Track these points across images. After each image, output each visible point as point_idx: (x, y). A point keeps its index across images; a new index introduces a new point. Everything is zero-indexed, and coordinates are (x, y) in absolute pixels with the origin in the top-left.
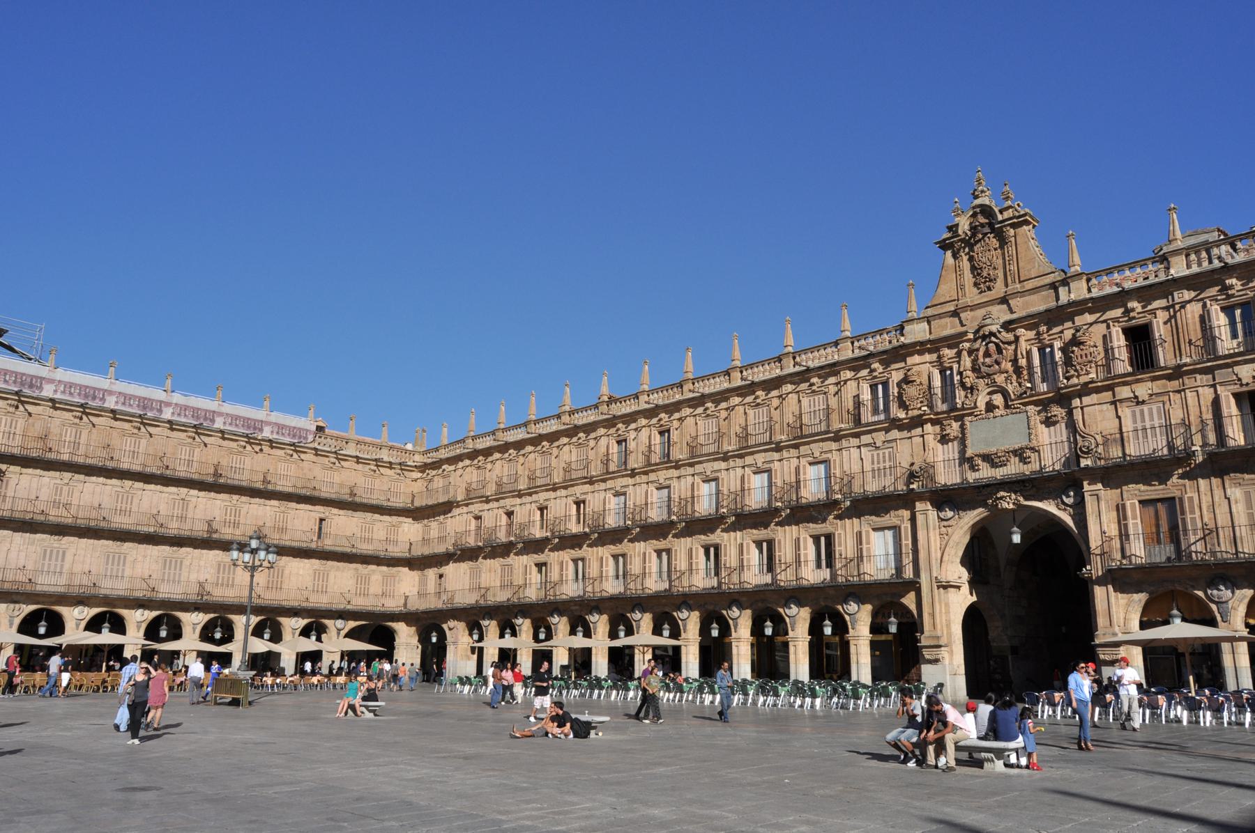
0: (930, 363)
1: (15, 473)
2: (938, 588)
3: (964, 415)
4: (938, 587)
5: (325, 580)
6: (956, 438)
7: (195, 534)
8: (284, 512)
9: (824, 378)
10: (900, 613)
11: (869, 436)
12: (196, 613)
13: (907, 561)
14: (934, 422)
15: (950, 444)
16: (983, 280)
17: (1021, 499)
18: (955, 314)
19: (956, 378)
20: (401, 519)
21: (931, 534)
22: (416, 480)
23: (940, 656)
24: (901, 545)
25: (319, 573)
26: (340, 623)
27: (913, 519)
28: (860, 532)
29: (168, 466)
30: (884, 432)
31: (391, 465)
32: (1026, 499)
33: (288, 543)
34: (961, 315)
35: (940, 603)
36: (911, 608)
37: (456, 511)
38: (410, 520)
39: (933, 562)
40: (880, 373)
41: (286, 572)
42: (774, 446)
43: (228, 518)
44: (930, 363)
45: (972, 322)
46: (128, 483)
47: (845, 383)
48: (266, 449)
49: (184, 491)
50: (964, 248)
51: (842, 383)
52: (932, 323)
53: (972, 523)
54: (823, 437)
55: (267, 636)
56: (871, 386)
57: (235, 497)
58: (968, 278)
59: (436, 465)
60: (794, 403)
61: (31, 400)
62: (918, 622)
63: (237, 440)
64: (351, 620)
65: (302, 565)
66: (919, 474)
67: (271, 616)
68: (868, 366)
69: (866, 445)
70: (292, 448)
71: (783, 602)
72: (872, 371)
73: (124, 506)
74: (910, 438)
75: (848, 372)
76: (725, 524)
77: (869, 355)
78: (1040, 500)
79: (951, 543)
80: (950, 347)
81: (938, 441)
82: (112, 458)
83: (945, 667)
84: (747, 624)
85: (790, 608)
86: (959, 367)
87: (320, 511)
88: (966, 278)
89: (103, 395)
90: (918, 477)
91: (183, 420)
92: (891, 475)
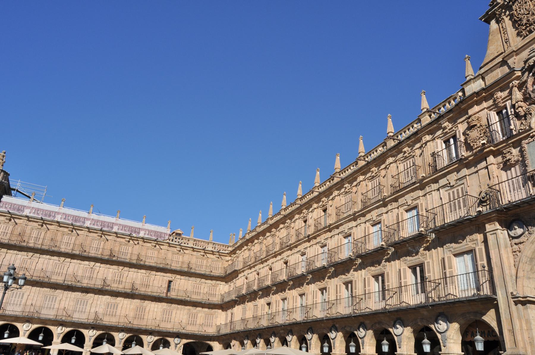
0: (487, 108)
1: (4, 252)
2: (516, 305)
3: (521, 139)
4: (516, 303)
5: (170, 315)
6: (517, 162)
7: (96, 287)
8: (148, 276)
9: (411, 146)
10: (486, 332)
11: (445, 179)
12: (92, 330)
13: (484, 278)
14: (496, 154)
15: (513, 169)
16: (524, 28)
18: (504, 63)
19: (511, 111)
20: (218, 282)
21: (503, 252)
22: (228, 261)
24: (477, 265)
25: (167, 311)
26: (177, 340)
27: (485, 241)
28: (443, 259)
29: (85, 251)
30: (456, 173)
31: (213, 253)
33: (149, 294)
34: (509, 62)
35: (520, 319)
36: (492, 326)
37: (240, 275)
38: (224, 283)
39: (508, 278)
40: (449, 130)
41: (147, 310)
42: (382, 202)
43: (116, 278)
44: (487, 108)
45: (519, 63)
46: (62, 259)
47: (426, 145)
48: (141, 243)
49: (92, 263)
50: (505, 12)
51: (424, 146)
52: (486, 78)
54: (412, 187)
55: (73, 341)
56: (445, 142)
57: (121, 268)
58: (511, 31)
59: (233, 252)
60: (395, 170)
61: (17, 217)
62: (501, 340)
63: (125, 238)
64: (184, 339)
65: (156, 306)
66: (486, 199)
67: (136, 334)
68: (439, 128)
69: (443, 187)
70: (156, 242)
71: (393, 323)
72: (445, 128)
73: (59, 270)
74: (477, 172)
75: (427, 136)
76: (355, 266)
77: (439, 117)
79: (524, 259)
80: (502, 90)
81: (502, 169)
82: (56, 246)
84: (371, 342)
85: (397, 328)
86: (512, 101)
87: (169, 276)
88: (509, 32)
89: (55, 214)
90: (485, 202)
91: (96, 227)
92: (465, 206)
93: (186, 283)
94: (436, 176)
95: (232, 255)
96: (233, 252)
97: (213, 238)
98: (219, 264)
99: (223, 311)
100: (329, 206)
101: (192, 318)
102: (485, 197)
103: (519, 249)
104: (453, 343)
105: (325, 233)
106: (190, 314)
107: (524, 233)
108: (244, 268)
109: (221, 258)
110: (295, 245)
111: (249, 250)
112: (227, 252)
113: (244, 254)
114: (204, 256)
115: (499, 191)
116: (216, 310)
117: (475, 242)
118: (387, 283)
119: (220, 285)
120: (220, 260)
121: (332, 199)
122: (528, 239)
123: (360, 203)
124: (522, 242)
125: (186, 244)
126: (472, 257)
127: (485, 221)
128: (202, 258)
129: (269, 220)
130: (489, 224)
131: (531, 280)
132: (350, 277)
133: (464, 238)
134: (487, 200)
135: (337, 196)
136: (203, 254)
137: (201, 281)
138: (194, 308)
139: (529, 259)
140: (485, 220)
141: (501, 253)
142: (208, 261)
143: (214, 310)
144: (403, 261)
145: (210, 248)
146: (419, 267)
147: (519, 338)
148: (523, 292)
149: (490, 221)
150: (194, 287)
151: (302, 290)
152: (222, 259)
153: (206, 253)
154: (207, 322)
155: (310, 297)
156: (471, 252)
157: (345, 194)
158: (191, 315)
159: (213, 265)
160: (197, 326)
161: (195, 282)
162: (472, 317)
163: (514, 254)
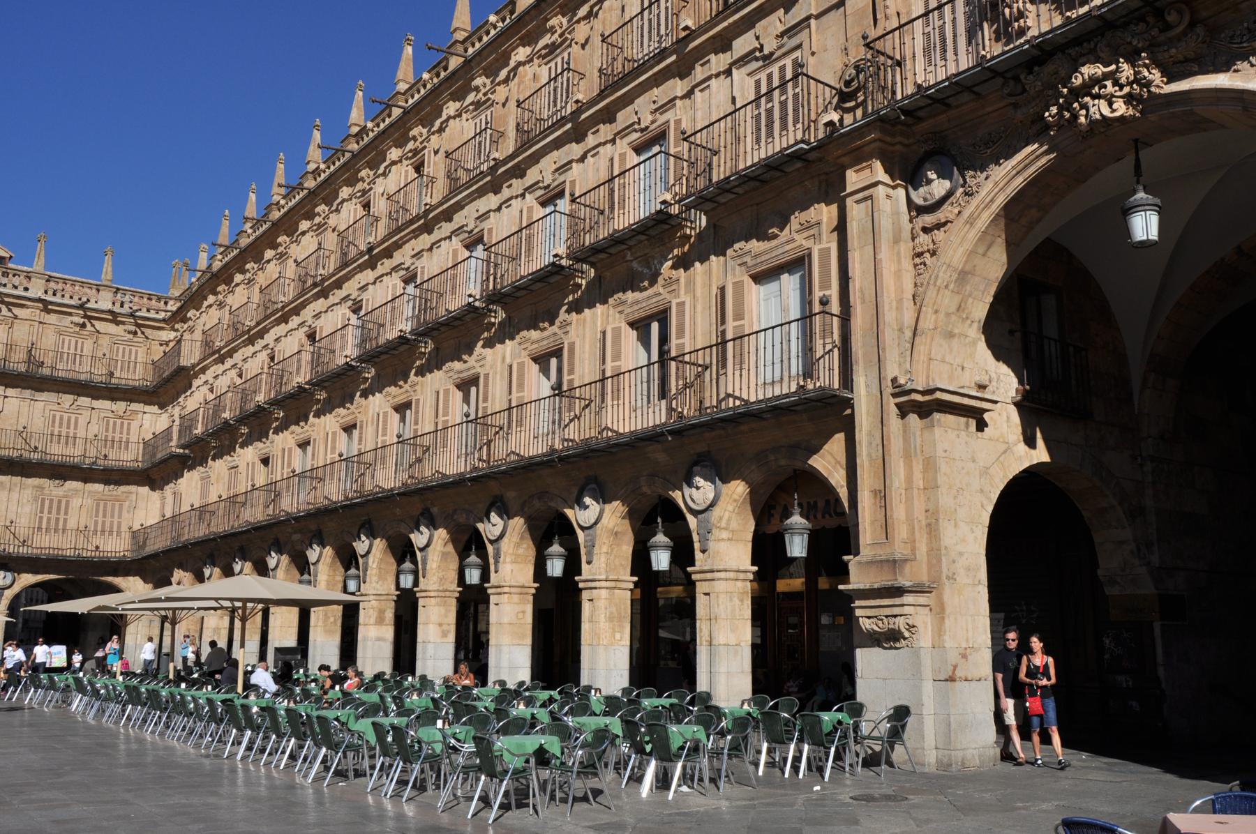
2: (903, 415)
4: (903, 411)
10: (821, 504)
11: (749, 36)
17: (1155, 76)
21: (884, 254)
23: (900, 623)
30: (782, 11)
31: (114, 318)
32: (1171, 76)
35: (908, 457)
36: (833, 482)
37: (196, 383)
38: (155, 409)
39: (889, 336)
42: (569, 126)
53: (1001, 200)
62: (850, 524)
64: (27, 572)
71: (575, 491)
76: (489, 330)
78: (1225, 67)
83: (917, 653)
84: (521, 551)
85: (586, 507)
92: (796, 121)
93: (27, 409)
94: (725, 24)
95: (177, 326)
96: (179, 317)
97: (114, 271)
98: (136, 353)
99: (153, 489)
100: (429, 152)
101: (50, 512)
102: (852, 80)
103: (931, 246)
104: (729, 539)
105: (416, 237)
106: (43, 500)
107: (953, 194)
108: (204, 359)
109: (143, 333)
110: (334, 279)
111: (221, 305)
112: (162, 315)
113: (208, 318)
114: (83, 326)
115: (899, 64)
116: (133, 488)
117: (812, 232)
118: (569, 375)
119: (140, 415)
120: (141, 340)
121: (441, 130)
122: (960, 212)
123: (511, 133)
124: (943, 221)
125: (21, 288)
126: (802, 278)
127: (845, 160)
128: (78, 333)
129: (271, 211)
130: (857, 168)
131: (955, 342)
132: (475, 364)
133: (783, 222)
134: (858, 90)
135: (454, 117)
136: (82, 321)
137: (76, 403)
138: (57, 481)
139: (955, 276)
140: (844, 155)
141: (878, 257)
142: (99, 342)
143: (123, 488)
144: (615, 306)
145: (104, 302)
146: (658, 321)
147: (899, 512)
148: (928, 377)
149: (859, 158)
150: (54, 422)
151: (348, 415)
152: (147, 338)
153: (90, 318)
154: (104, 522)
155: (369, 432)
156: (798, 264)
157: (475, 110)
158: (47, 503)
159: (117, 355)
160: (71, 535)
161: (56, 407)
162: (783, 462)
163: (917, 260)
